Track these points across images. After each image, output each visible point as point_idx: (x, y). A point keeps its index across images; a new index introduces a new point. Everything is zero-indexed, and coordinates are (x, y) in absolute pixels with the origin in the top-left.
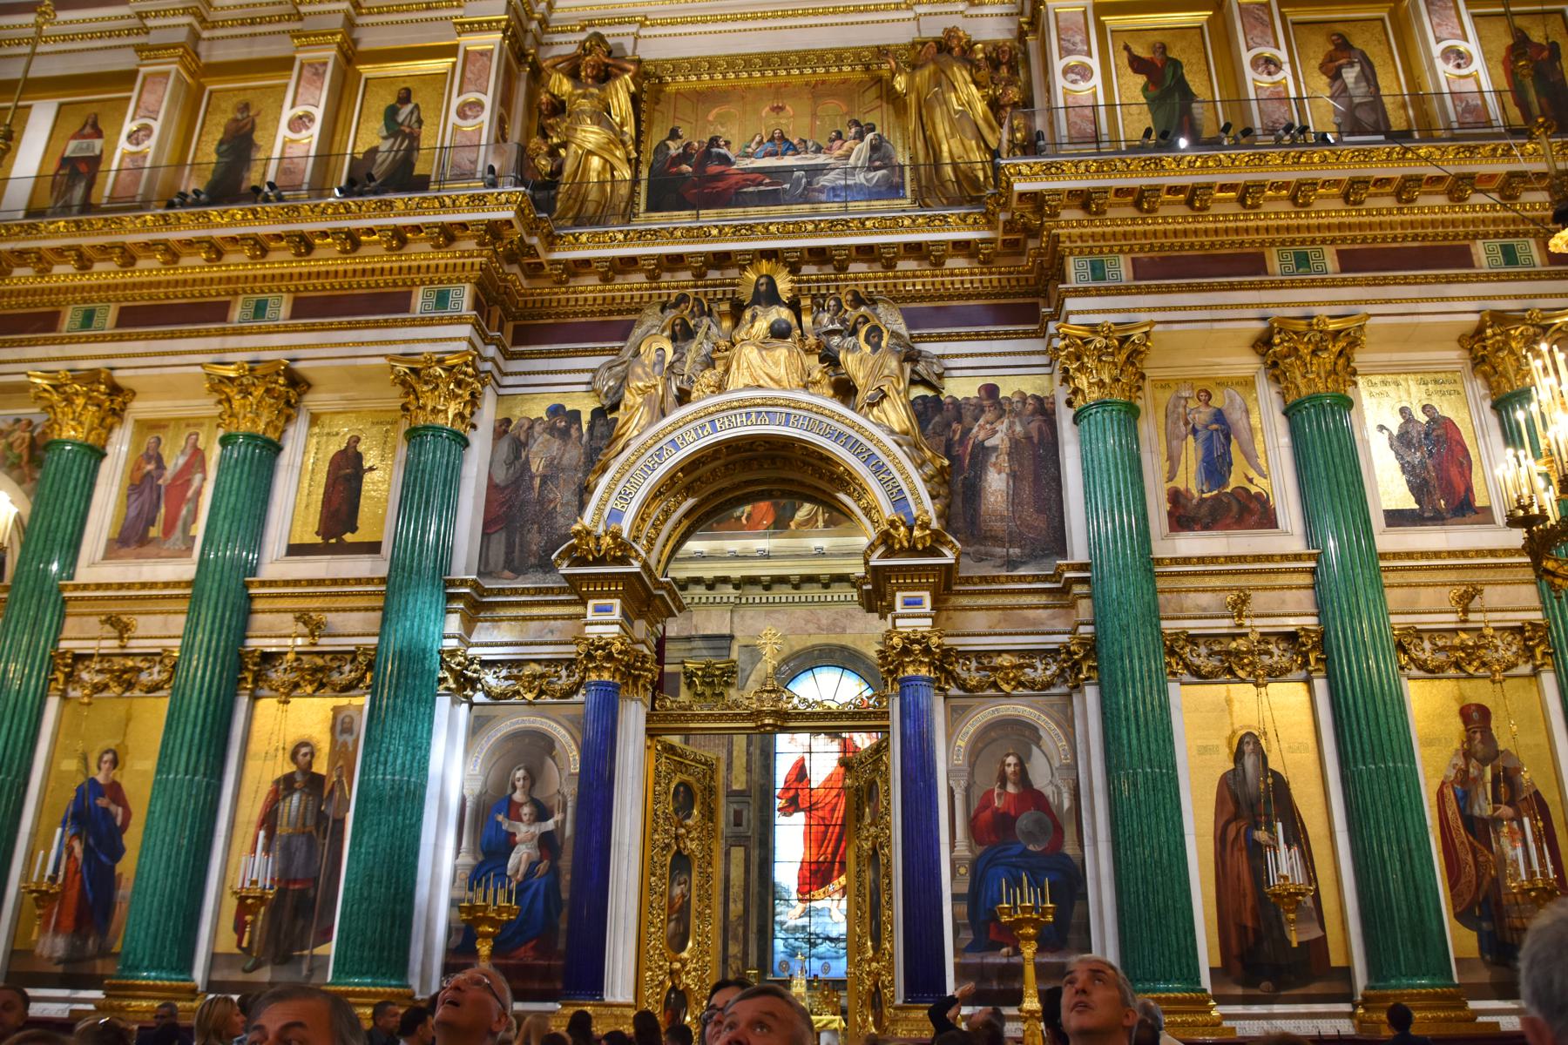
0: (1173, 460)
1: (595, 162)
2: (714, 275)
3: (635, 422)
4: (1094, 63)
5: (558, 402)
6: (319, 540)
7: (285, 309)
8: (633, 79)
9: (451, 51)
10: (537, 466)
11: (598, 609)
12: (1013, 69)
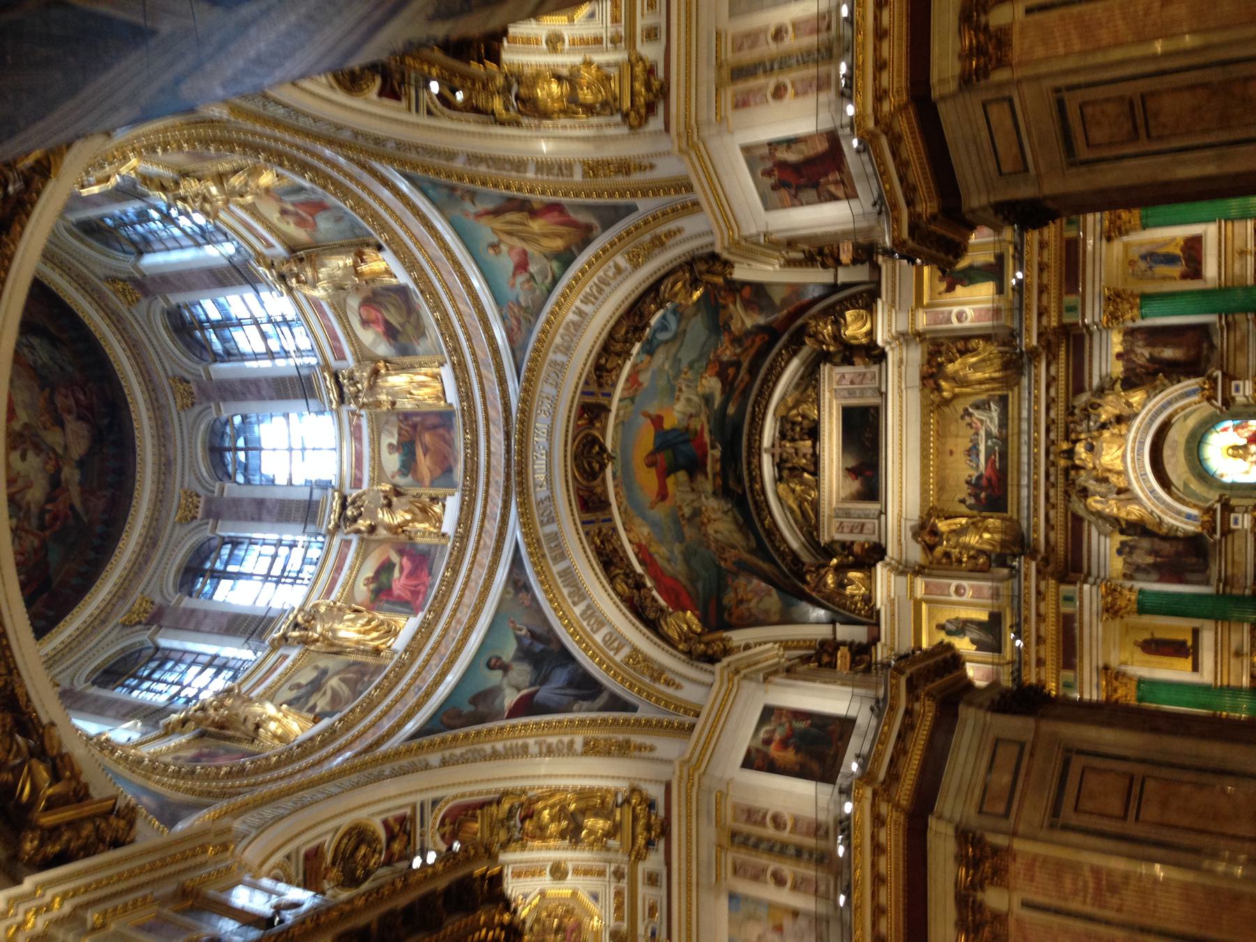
0: (1164, 278)
1: (986, 536)
2: (1052, 479)
3: (1133, 512)
4: (956, 309)
5: (1114, 550)
6: (1190, 659)
7: (1068, 675)
8: (938, 517)
9: (917, 604)
10: (1150, 560)
11: (1236, 522)
12: (942, 344)
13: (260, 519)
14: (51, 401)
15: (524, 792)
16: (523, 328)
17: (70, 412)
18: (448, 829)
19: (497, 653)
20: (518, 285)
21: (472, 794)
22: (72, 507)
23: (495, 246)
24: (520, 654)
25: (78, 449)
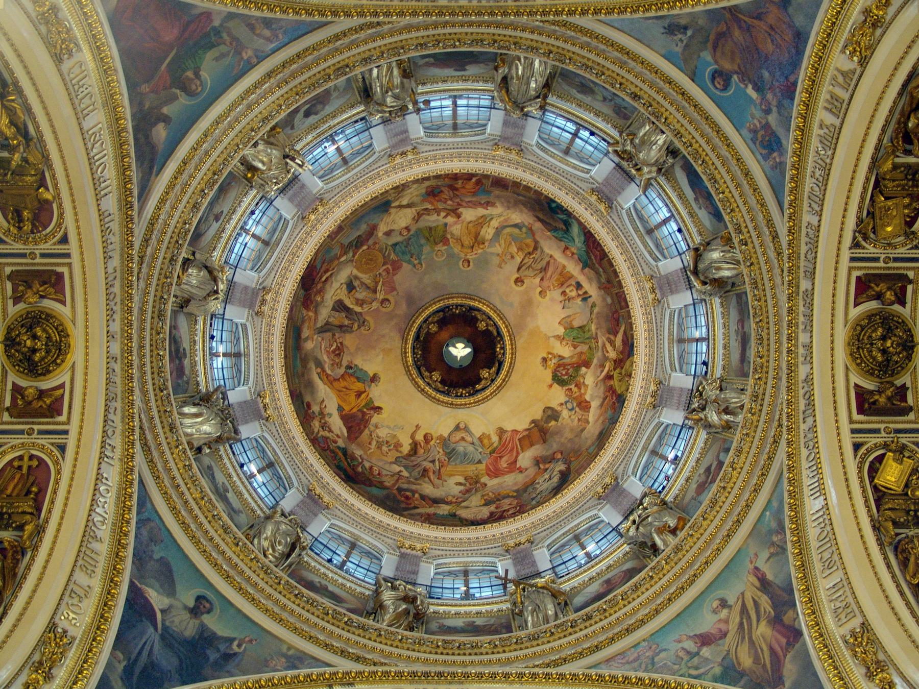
13: (397, 569)
14: (508, 496)
15: (36, 548)
16: (627, 666)
17: (497, 508)
18: (26, 463)
19: (217, 610)
20: (680, 645)
21: (55, 492)
22: (415, 508)
23: (724, 604)
24: (206, 635)
25: (464, 513)
